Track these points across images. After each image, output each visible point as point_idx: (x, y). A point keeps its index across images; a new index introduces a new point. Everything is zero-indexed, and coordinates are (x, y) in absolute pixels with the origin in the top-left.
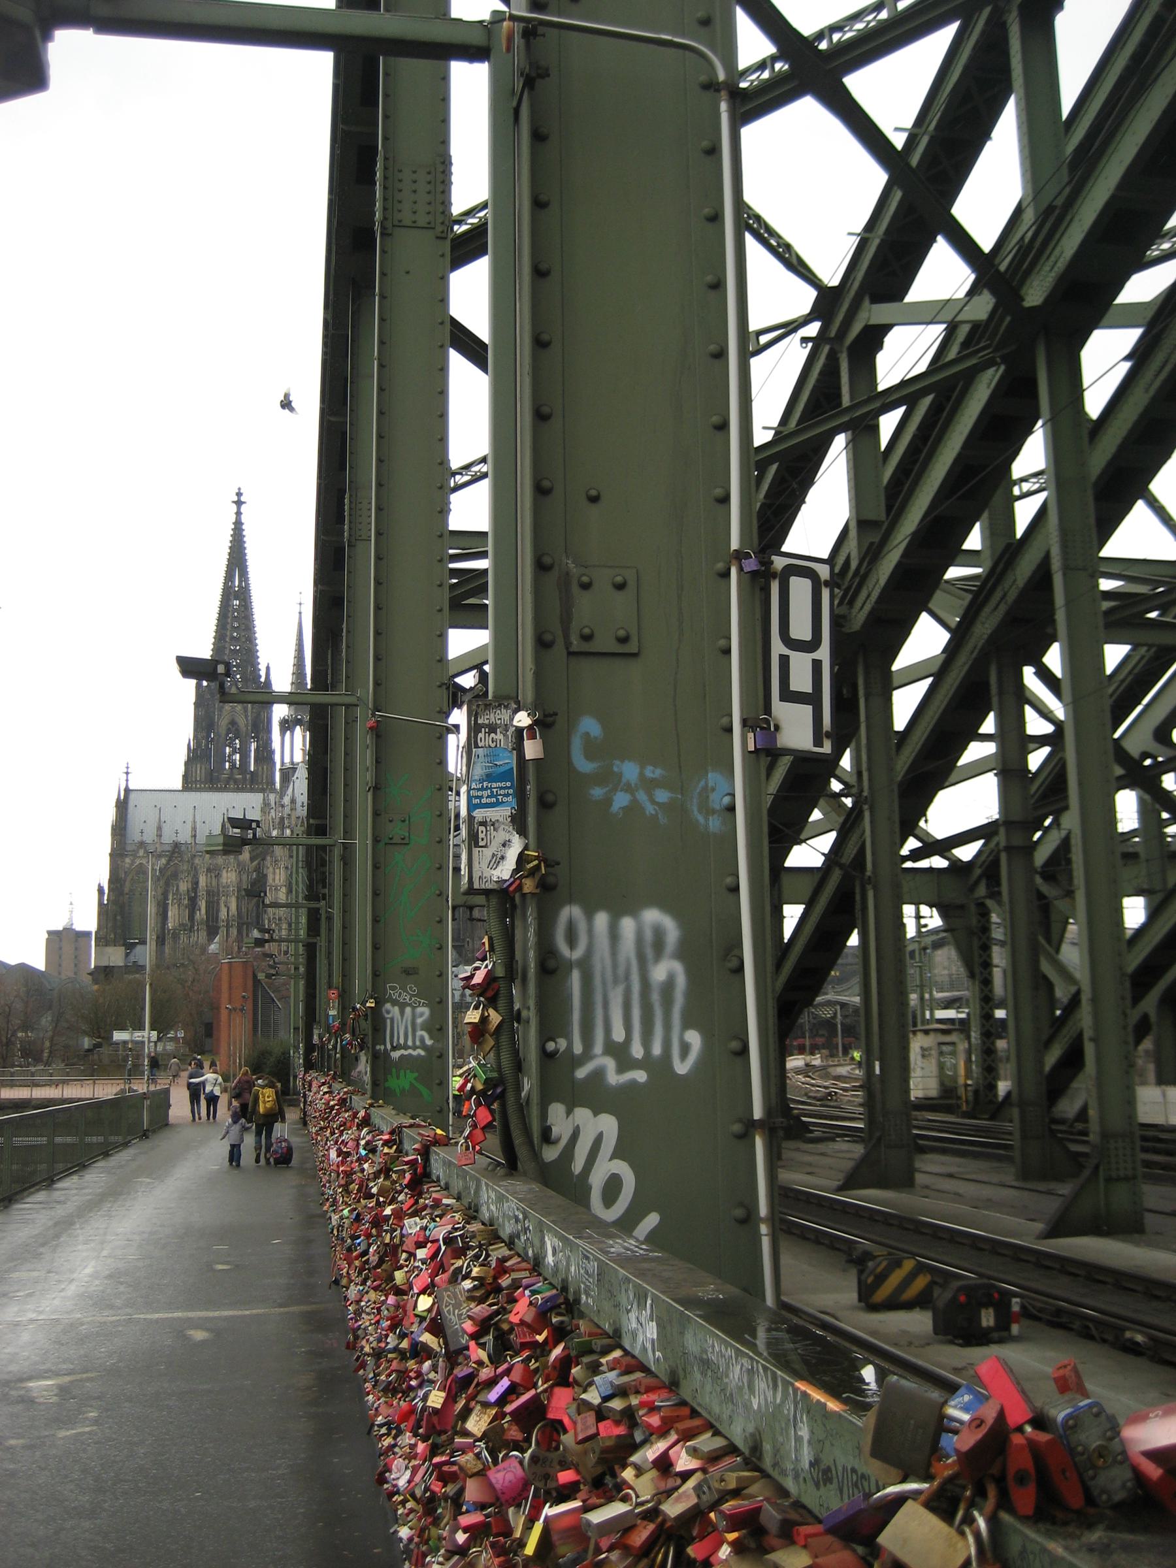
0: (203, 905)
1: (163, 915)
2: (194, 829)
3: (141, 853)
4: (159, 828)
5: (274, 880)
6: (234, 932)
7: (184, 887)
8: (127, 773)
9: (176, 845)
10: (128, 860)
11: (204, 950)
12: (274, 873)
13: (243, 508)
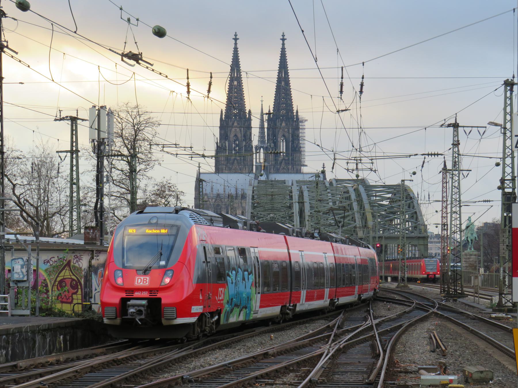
4: (212, 188)
9: (218, 195)
13: (238, 41)
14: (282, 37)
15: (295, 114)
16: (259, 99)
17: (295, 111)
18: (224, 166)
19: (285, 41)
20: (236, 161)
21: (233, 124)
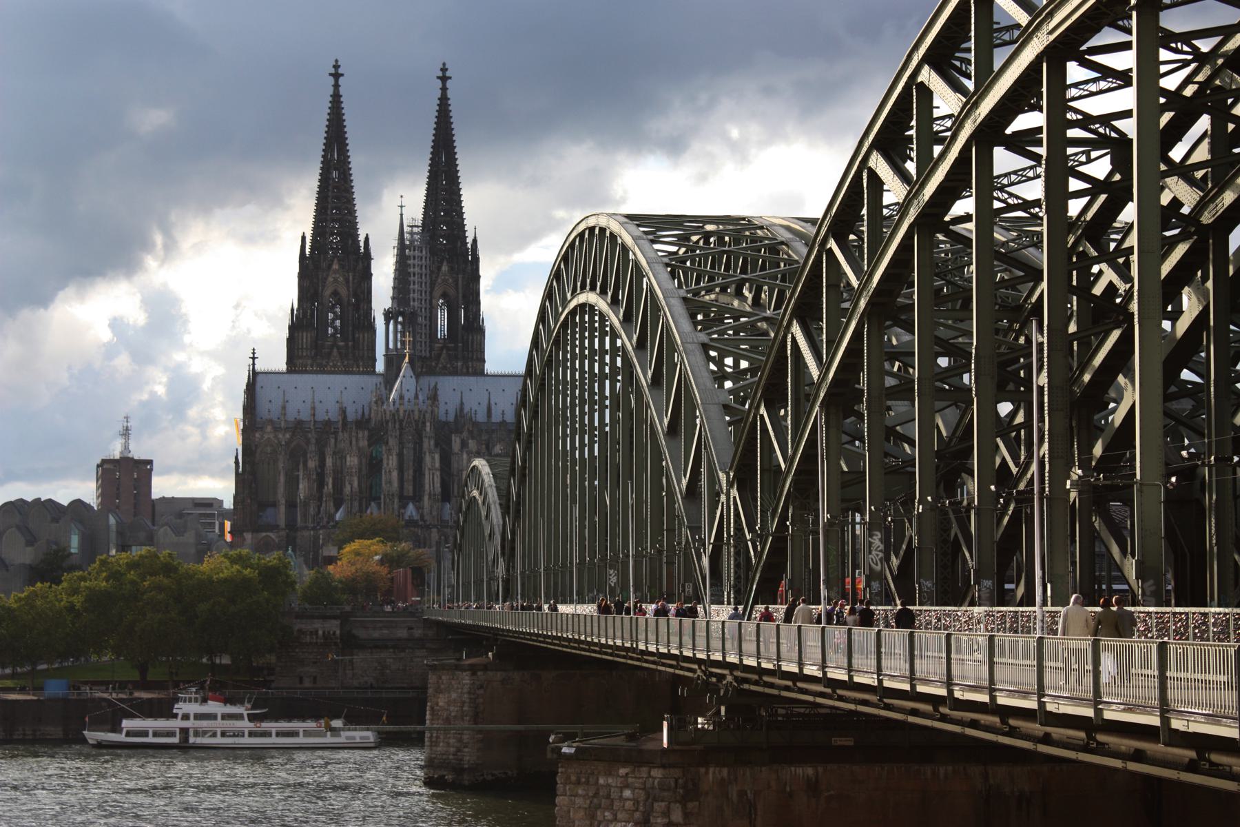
1: (292, 482)
2: (313, 408)
3: (269, 428)
4: (284, 408)
6: (356, 504)
7: (312, 464)
8: (254, 358)
9: (299, 424)
11: (331, 517)
13: (341, 80)
15: (469, 246)
17: (469, 240)
18: (309, 362)
21: (330, 266)
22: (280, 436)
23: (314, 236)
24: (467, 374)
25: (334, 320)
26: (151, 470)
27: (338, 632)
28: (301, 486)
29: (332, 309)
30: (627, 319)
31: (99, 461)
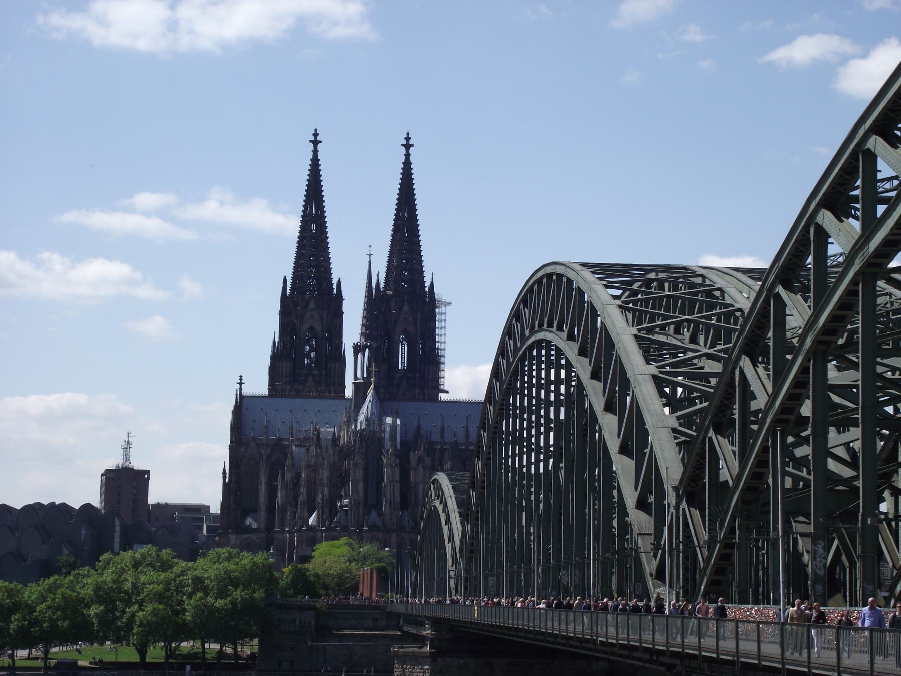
0: (303, 490)
2: (292, 427)
3: (253, 444)
5: (355, 476)
6: (327, 510)
7: (288, 476)
8: (241, 383)
10: (242, 450)
12: (355, 472)
14: (405, 142)
15: (427, 289)
16: (358, 261)
17: (428, 285)
19: (412, 150)
20: (310, 377)
21: (307, 305)
22: (263, 451)
23: (293, 279)
24: (424, 400)
25: (310, 351)
26: (148, 478)
27: (313, 622)
28: (279, 495)
29: (308, 342)
30: (582, 352)
31: (103, 471)
